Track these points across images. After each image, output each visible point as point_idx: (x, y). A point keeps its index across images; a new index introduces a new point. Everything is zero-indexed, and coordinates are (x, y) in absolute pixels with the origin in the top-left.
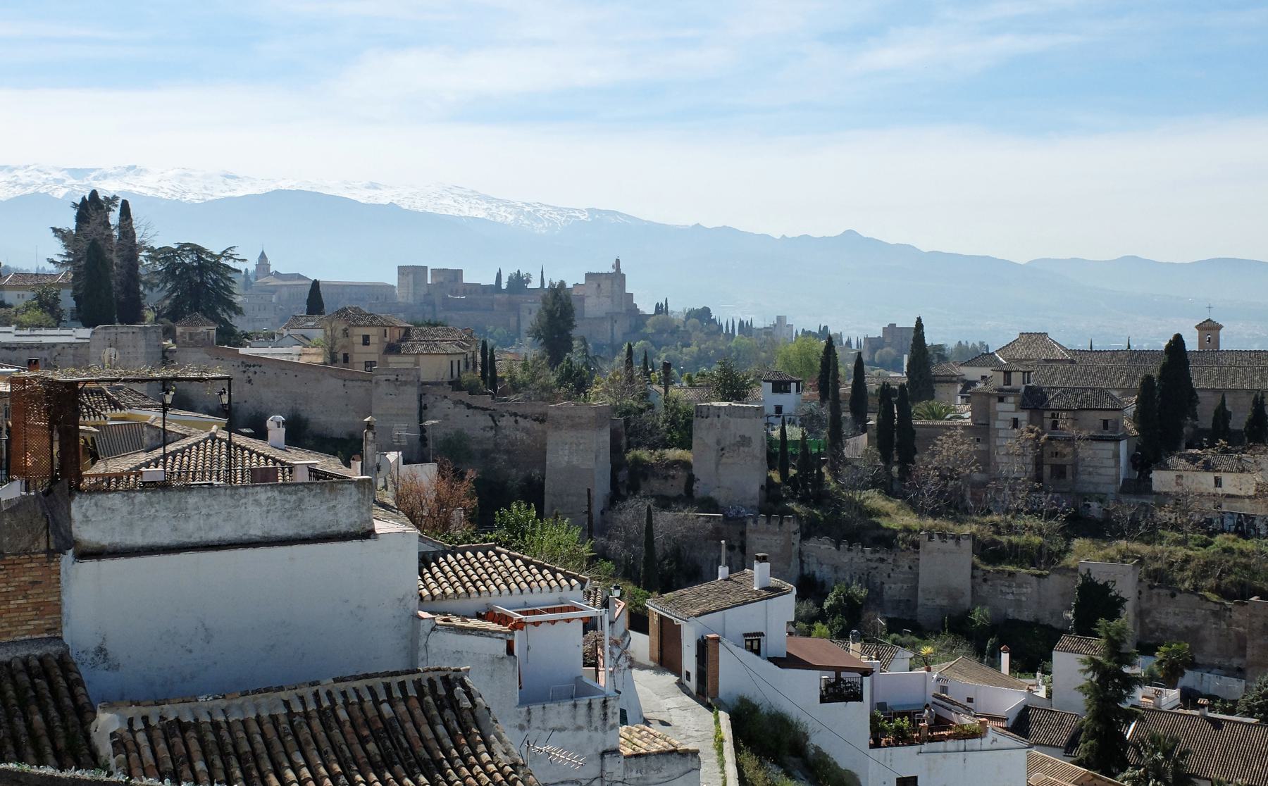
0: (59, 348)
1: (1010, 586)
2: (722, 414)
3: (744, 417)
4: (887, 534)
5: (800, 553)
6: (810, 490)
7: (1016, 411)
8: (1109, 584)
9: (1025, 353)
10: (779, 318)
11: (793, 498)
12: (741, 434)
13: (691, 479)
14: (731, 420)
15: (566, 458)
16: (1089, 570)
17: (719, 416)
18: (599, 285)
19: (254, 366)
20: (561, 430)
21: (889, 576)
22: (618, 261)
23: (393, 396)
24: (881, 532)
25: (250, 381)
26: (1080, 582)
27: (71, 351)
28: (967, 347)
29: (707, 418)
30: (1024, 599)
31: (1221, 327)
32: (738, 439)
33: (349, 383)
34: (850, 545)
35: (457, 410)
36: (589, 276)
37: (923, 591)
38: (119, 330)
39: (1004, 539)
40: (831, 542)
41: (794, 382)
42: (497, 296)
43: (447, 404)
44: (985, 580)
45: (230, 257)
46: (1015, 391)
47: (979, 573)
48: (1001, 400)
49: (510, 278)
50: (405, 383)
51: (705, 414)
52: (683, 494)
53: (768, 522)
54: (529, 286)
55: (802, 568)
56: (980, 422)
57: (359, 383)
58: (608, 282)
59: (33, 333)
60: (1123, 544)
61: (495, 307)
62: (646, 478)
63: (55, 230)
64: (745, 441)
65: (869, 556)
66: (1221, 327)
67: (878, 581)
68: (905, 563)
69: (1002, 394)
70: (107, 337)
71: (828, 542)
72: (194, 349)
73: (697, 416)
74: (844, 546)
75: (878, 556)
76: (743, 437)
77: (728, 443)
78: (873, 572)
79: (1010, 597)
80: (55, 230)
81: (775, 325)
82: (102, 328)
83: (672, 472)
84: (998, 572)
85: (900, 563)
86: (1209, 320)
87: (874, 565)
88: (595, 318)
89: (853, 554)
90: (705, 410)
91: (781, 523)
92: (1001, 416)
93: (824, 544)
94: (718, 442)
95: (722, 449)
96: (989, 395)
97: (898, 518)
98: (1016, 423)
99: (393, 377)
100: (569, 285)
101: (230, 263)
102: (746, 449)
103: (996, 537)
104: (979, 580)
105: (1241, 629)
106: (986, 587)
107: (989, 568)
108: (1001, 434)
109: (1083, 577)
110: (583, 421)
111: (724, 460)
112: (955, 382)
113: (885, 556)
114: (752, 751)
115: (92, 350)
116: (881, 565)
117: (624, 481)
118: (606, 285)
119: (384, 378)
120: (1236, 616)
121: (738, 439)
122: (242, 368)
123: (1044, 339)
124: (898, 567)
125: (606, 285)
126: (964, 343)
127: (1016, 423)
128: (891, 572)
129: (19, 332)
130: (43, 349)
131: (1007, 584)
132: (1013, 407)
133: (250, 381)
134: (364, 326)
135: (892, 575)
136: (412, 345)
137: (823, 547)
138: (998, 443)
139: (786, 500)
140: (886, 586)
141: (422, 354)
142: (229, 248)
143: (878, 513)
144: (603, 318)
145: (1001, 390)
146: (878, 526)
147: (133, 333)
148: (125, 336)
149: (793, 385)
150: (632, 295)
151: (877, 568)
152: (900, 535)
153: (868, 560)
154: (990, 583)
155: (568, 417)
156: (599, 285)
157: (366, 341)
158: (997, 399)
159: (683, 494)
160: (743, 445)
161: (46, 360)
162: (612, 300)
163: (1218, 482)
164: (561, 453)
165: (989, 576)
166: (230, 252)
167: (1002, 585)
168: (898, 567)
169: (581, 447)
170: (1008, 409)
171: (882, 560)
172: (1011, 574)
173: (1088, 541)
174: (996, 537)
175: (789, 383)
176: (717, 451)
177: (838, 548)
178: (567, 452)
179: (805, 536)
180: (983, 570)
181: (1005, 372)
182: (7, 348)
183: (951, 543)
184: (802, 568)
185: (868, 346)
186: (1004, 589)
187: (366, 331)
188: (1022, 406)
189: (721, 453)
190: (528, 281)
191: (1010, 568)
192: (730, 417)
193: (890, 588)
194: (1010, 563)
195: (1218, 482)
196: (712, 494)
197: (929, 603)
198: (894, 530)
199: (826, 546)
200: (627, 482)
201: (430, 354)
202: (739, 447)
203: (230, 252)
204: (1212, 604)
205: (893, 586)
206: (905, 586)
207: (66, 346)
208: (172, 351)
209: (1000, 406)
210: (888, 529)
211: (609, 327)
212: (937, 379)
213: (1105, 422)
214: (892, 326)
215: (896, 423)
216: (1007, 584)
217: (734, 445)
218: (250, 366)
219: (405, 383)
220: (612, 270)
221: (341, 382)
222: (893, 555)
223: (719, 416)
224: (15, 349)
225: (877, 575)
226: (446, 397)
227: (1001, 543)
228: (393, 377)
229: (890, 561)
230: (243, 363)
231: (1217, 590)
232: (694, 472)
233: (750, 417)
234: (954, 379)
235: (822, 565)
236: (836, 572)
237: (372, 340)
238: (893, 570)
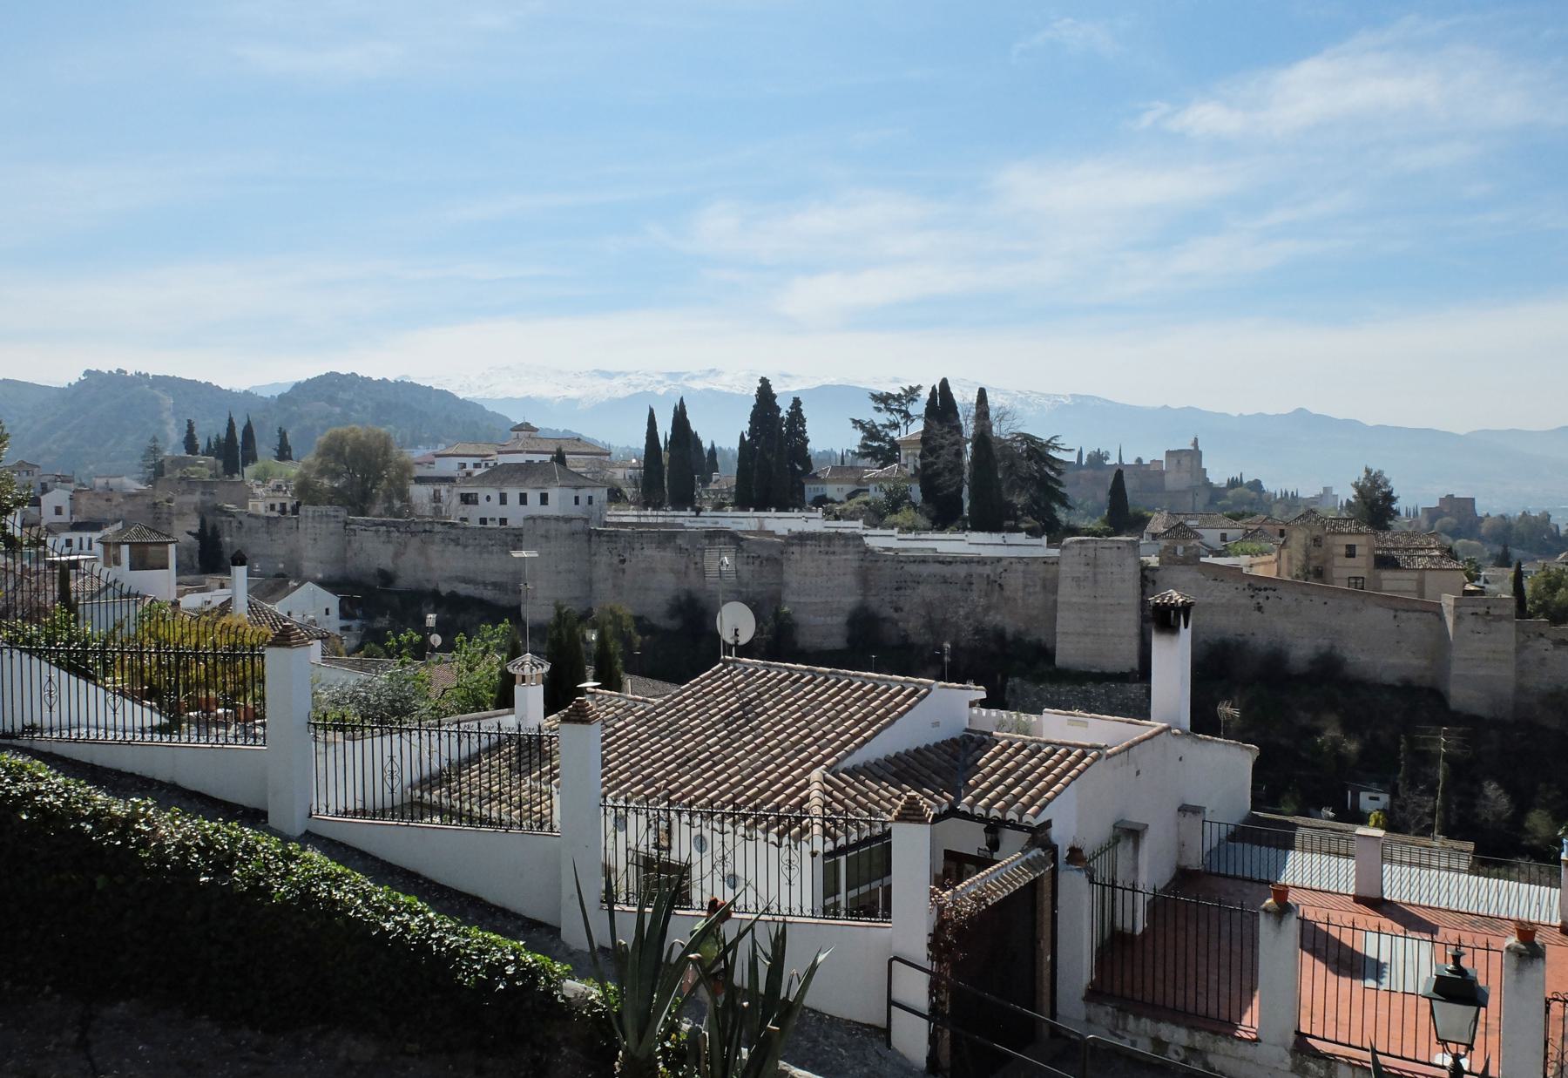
0: (1005, 563)
10: (1325, 489)
18: (1179, 462)
19: (1266, 589)
22: (1196, 440)
23: (1481, 635)
25: (1259, 608)
27: (1021, 567)
33: (1404, 615)
35: (1557, 652)
36: (1169, 453)
38: (1100, 545)
42: (1083, 472)
43: (1544, 644)
45: (1055, 447)
49: (1089, 456)
50: (1500, 618)
54: (1108, 463)
57: (1417, 615)
58: (1189, 458)
59: (918, 537)
61: (1082, 481)
63: (854, 421)
70: (1083, 553)
72: (1186, 567)
80: (854, 421)
81: (1321, 496)
82: (1077, 542)
88: (1179, 491)
99: (1482, 610)
100: (1146, 461)
101: (1053, 453)
115: (1063, 568)
118: (1185, 461)
119: (1471, 610)
122: (1250, 592)
125: (1185, 461)
129: (902, 536)
130: (986, 564)
133: (1259, 608)
134: (1350, 533)
136: (1409, 557)
141: (1430, 569)
142: (1052, 438)
144: (1184, 491)
147: (1119, 548)
148: (1107, 551)
150: (1205, 470)
156: (1179, 462)
157: (1351, 552)
161: (988, 576)
162: (1192, 476)
166: (1054, 441)
182: (940, 562)
185: (1426, 515)
187: (1351, 540)
190: (1107, 458)
201: (1441, 569)
203: (1054, 441)
207: (1013, 560)
208: (1154, 569)
211: (1191, 500)
218: (1260, 590)
219: (1500, 618)
220: (1192, 448)
221: (1392, 613)
224: (950, 563)
226: (1542, 635)
228: (1482, 610)
230: (1249, 585)
237: (1343, 550)
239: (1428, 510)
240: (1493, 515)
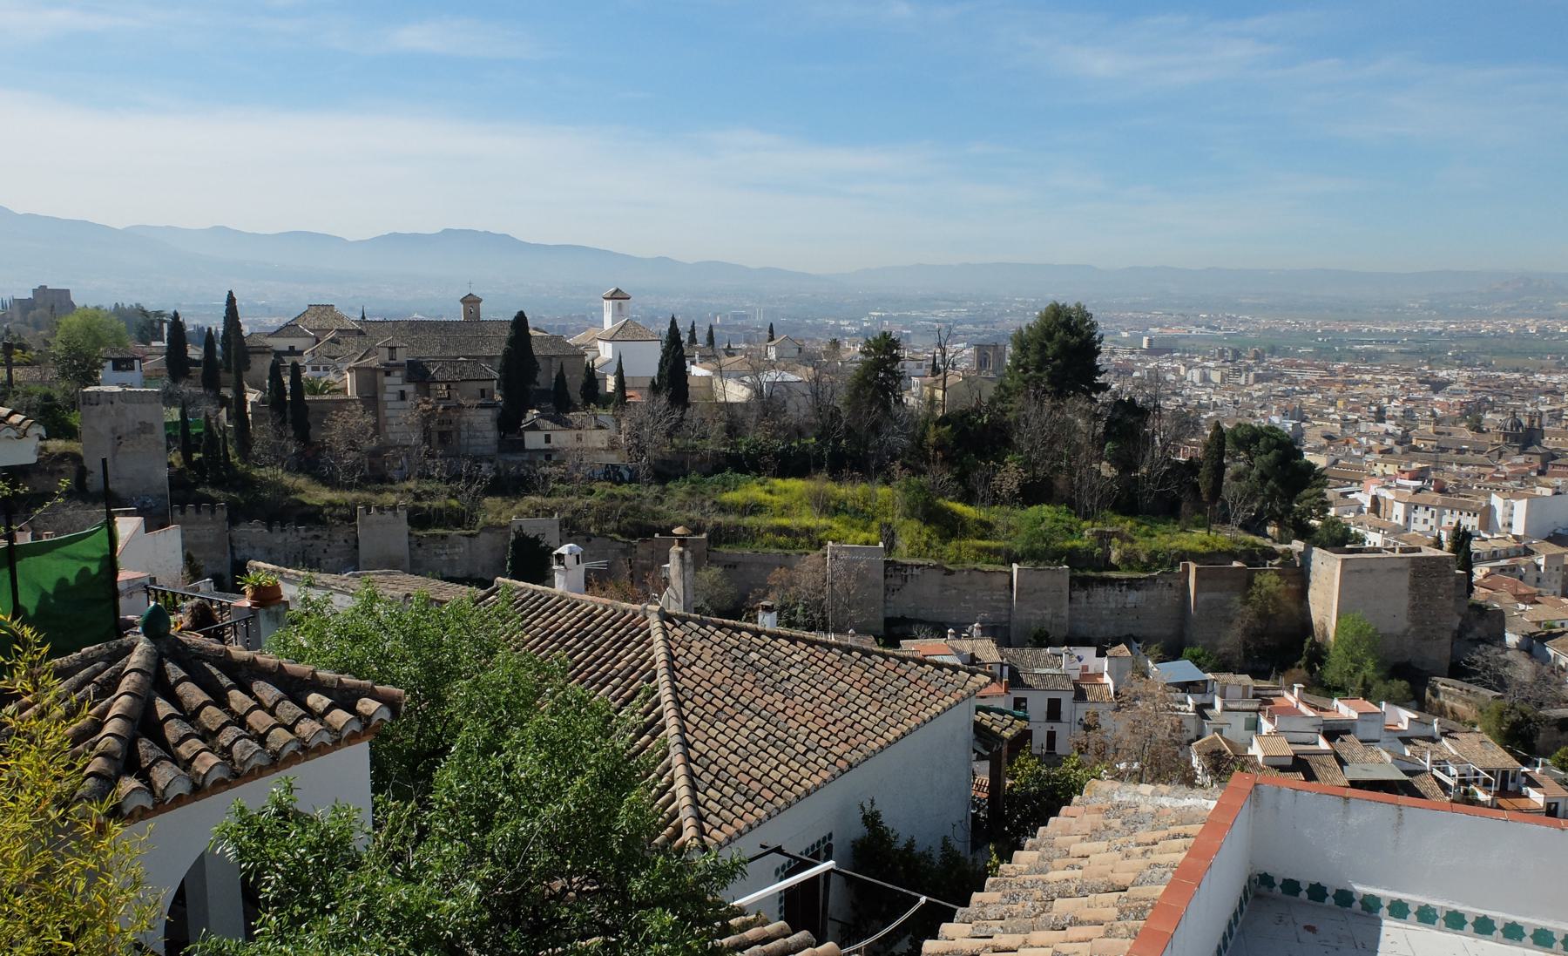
1: (443, 548)
2: (116, 400)
4: (312, 510)
5: (230, 538)
6: (224, 473)
9: (317, 323)
11: (204, 485)
12: (141, 420)
17: (112, 403)
21: (325, 551)
24: (306, 509)
26: (513, 537)
28: (123, 308)
29: (97, 404)
30: (457, 558)
31: (481, 300)
32: (138, 426)
34: (283, 525)
39: (425, 504)
44: (419, 545)
46: (399, 366)
47: (414, 539)
48: (388, 374)
52: (74, 488)
53: (198, 512)
55: (233, 554)
60: (533, 499)
64: (146, 428)
65: (302, 534)
66: (481, 300)
68: (340, 536)
69: (388, 369)
73: (84, 404)
74: (276, 528)
79: (444, 558)
83: (63, 467)
84: (431, 536)
85: (336, 538)
86: (470, 294)
89: (288, 534)
90: (94, 397)
91: (213, 512)
92: (389, 389)
93: (255, 527)
94: (113, 430)
96: (375, 370)
97: (320, 495)
102: (149, 436)
103: (417, 503)
104: (414, 546)
105: (645, 561)
106: (420, 552)
107: (421, 533)
109: (516, 533)
111: (122, 448)
112: (269, 353)
113: (319, 533)
114: (890, 843)
116: (316, 542)
120: (640, 551)
121: (138, 426)
123: (332, 311)
124: (333, 541)
126: (120, 304)
127: (402, 396)
132: (399, 381)
137: (254, 530)
138: (388, 413)
139: (196, 485)
145: (387, 365)
146: (303, 504)
149: (137, 362)
151: (311, 545)
152: (326, 511)
153: (303, 539)
154: (424, 547)
160: (144, 432)
168: (333, 541)
170: (394, 383)
171: (317, 537)
172: (443, 537)
173: (499, 499)
174: (417, 503)
175: (132, 360)
177: (270, 530)
179: (233, 521)
180: (417, 536)
181: (391, 348)
183: (389, 514)
184: (233, 554)
186: (438, 551)
188: (409, 380)
191: (440, 531)
194: (437, 526)
198: (318, 506)
204: (621, 544)
205: (330, 560)
206: (342, 559)
209: (387, 380)
210: (312, 506)
212: (250, 350)
213: (483, 391)
214: (43, 288)
215: (288, 398)
223: (112, 403)
227: (423, 508)
229: (325, 537)
231: (618, 531)
232: (86, 463)
233: (151, 403)
234: (267, 350)
235: (254, 548)
239: (21, 301)
240: (91, 304)
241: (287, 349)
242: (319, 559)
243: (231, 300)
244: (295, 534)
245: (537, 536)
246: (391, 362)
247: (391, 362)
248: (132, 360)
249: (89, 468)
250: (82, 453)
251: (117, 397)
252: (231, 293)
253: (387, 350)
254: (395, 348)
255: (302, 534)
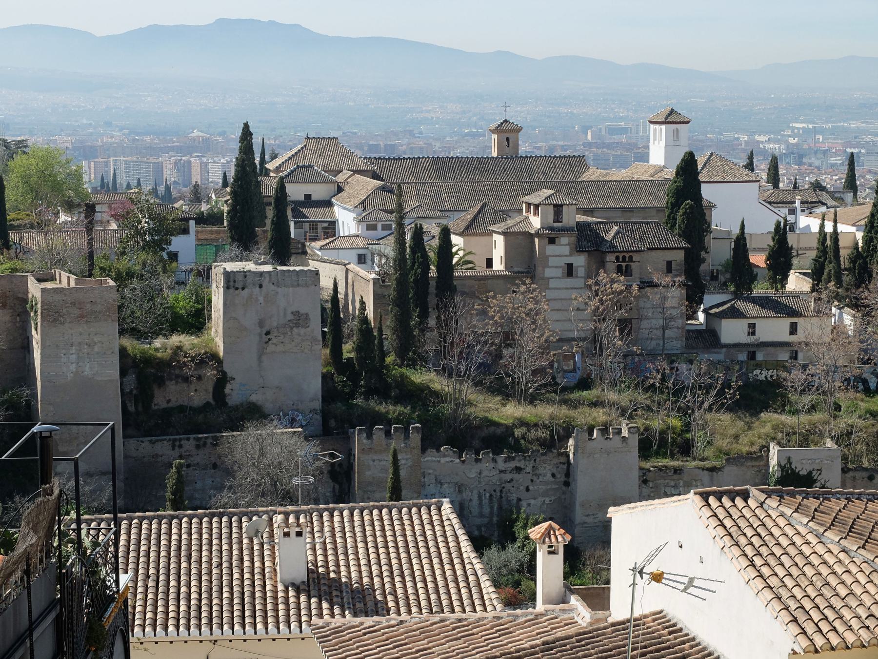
2: (266, 282)
3: (298, 285)
4: (499, 431)
7: (571, 255)
8: (814, 473)
13: (222, 381)
14: (279, 290)
15: (73, 367)
16: (789, 459)
17: (261, 286)
20: (63, 324)
21: (528, 489)
29: (243, 289)
32: (290, 317)
37: (582, 505)
40: (454, 452)
41: (193, 219)
46: (565, 230)
48: (552, 241)
51: (240, 285)
52: (212, 402)
56: (516, 269)
62: (161, 382)
67: (514, 497)
71: (451, 453)
75: (513, 464)
76: (296, 313)
77: (275, 324)
78: (508, 486)
84: (660, 469)
86: (505, 121)
87: (508, 477)
90: (240, 278)
92: (552, 261)
93: (445, 456)
94: (261, 324)
95: (268, 333)
98: (570, 270)
102: (302, 331)
108: (553, 284)
110: (98, 308)
111: (271, 348)
113: (521, 464)
116: (516, 476)
117: (131, 391)
124: (538, 476)
127: (570, 270)
128: (529, 483)
131: (672, 483)
132: (566, 250)
135: (531, 488)
137: (443, 460)
140: (524, 503)
143: (470, 403)
145: (551, 229)
151: (512, 480)
153: (501, 472)
154: (651, 484)
155: (73, 304)
158: (547, 240)
159: (212, 402)
160: (297, 325)
163: (793, 329)
164: (64, 360)
165: (649, 476)
167: (667, 486)
168: (538, 476)
169: (96, 349)
171: (518, 470)
172: (677, 471)
175: (187, 220)
176: (260, 335)
178: (73, 357)
181: (555, 206)
189: (265, 338)
192: (278, 287)
193: (529, 505)
195: (793, 329)
196: (254, 398)
197: (590, 520)
198: (507, 427)
199: (448, 459)
200: (135, 392)
202: (292, 328)
205: (532, 502)
206: (547, 500)
209: (551, 249)
212: (265, 200)
213: (669, 263)
216: (672, 483)
217: (284, 326)
222: (532, 461)
223: (261, 286)
225: (512, 490)
229: (529, 469)
232: (226, 368)
235: (442, 484)
236: (460, 491)
238: (532, 481)
241: (302, 198)
242: (519, 500)
243: (247, 134)
244: (492, 465)
245: (810, 473)
246: (556, 225)
247: (556, 225)
248: (187, 220)
249: (229, 375)
250: (221, 354)
251: (268, 279)
252: (246, 126)
253: (552, 207)
254: (561, 206)
255: (501, 465)
